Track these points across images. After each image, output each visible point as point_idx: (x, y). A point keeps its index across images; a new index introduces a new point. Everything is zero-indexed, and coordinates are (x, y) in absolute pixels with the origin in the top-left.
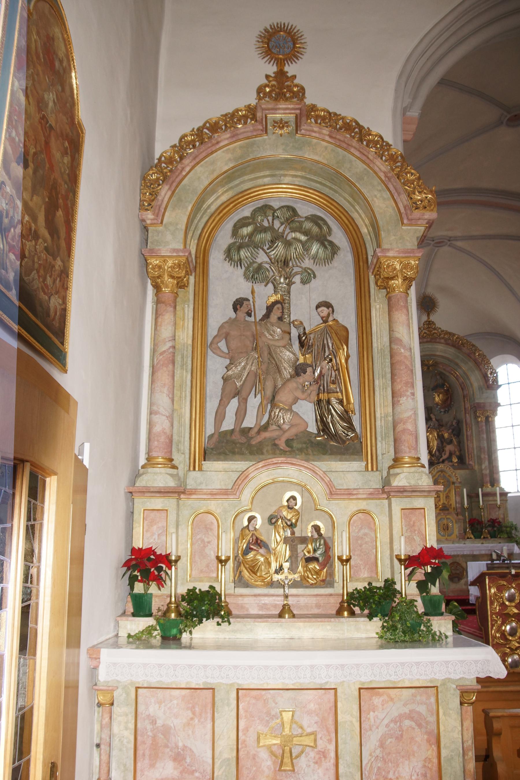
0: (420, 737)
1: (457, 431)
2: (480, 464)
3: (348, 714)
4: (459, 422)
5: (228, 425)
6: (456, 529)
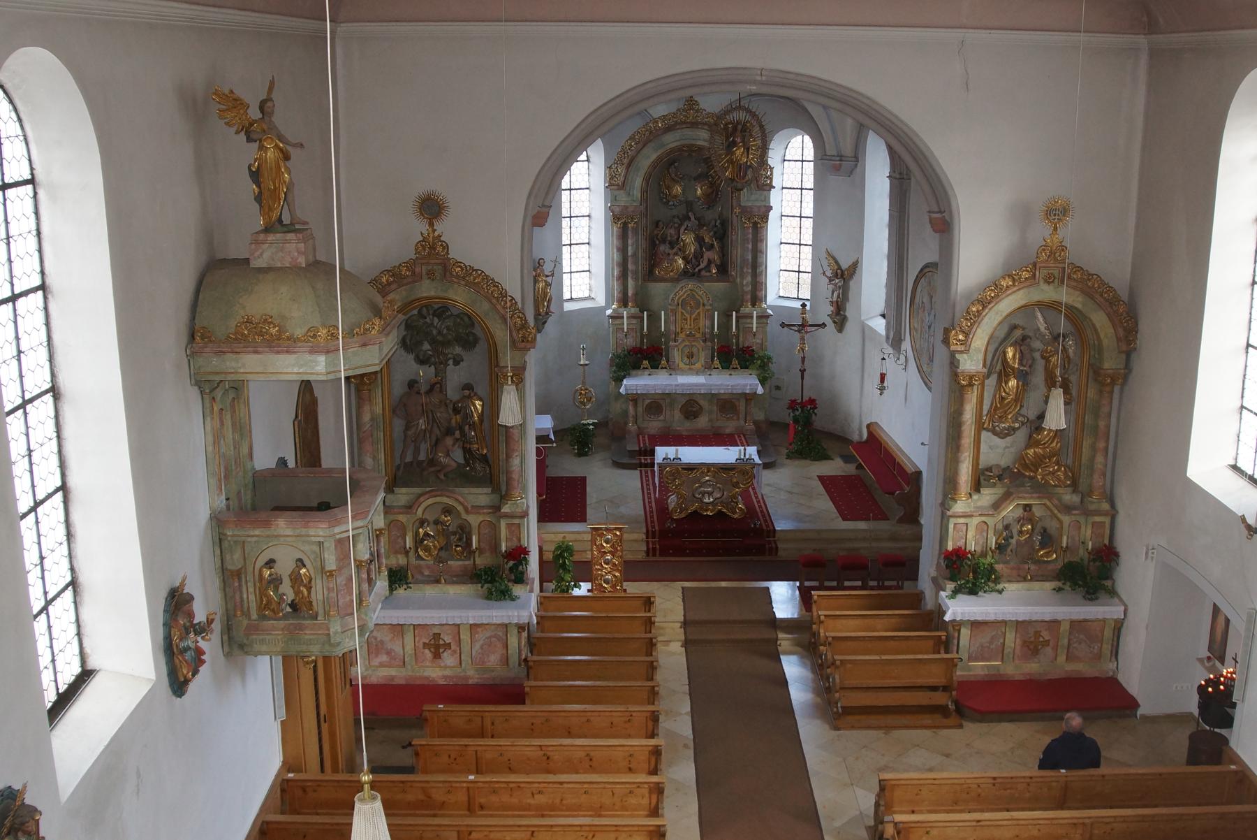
0: (499, 645)
1: (722, 234)
2: (742, 276)
3: (465, 636)
4: (724, 223)
5: (409, 459)
6: (702, 358)
